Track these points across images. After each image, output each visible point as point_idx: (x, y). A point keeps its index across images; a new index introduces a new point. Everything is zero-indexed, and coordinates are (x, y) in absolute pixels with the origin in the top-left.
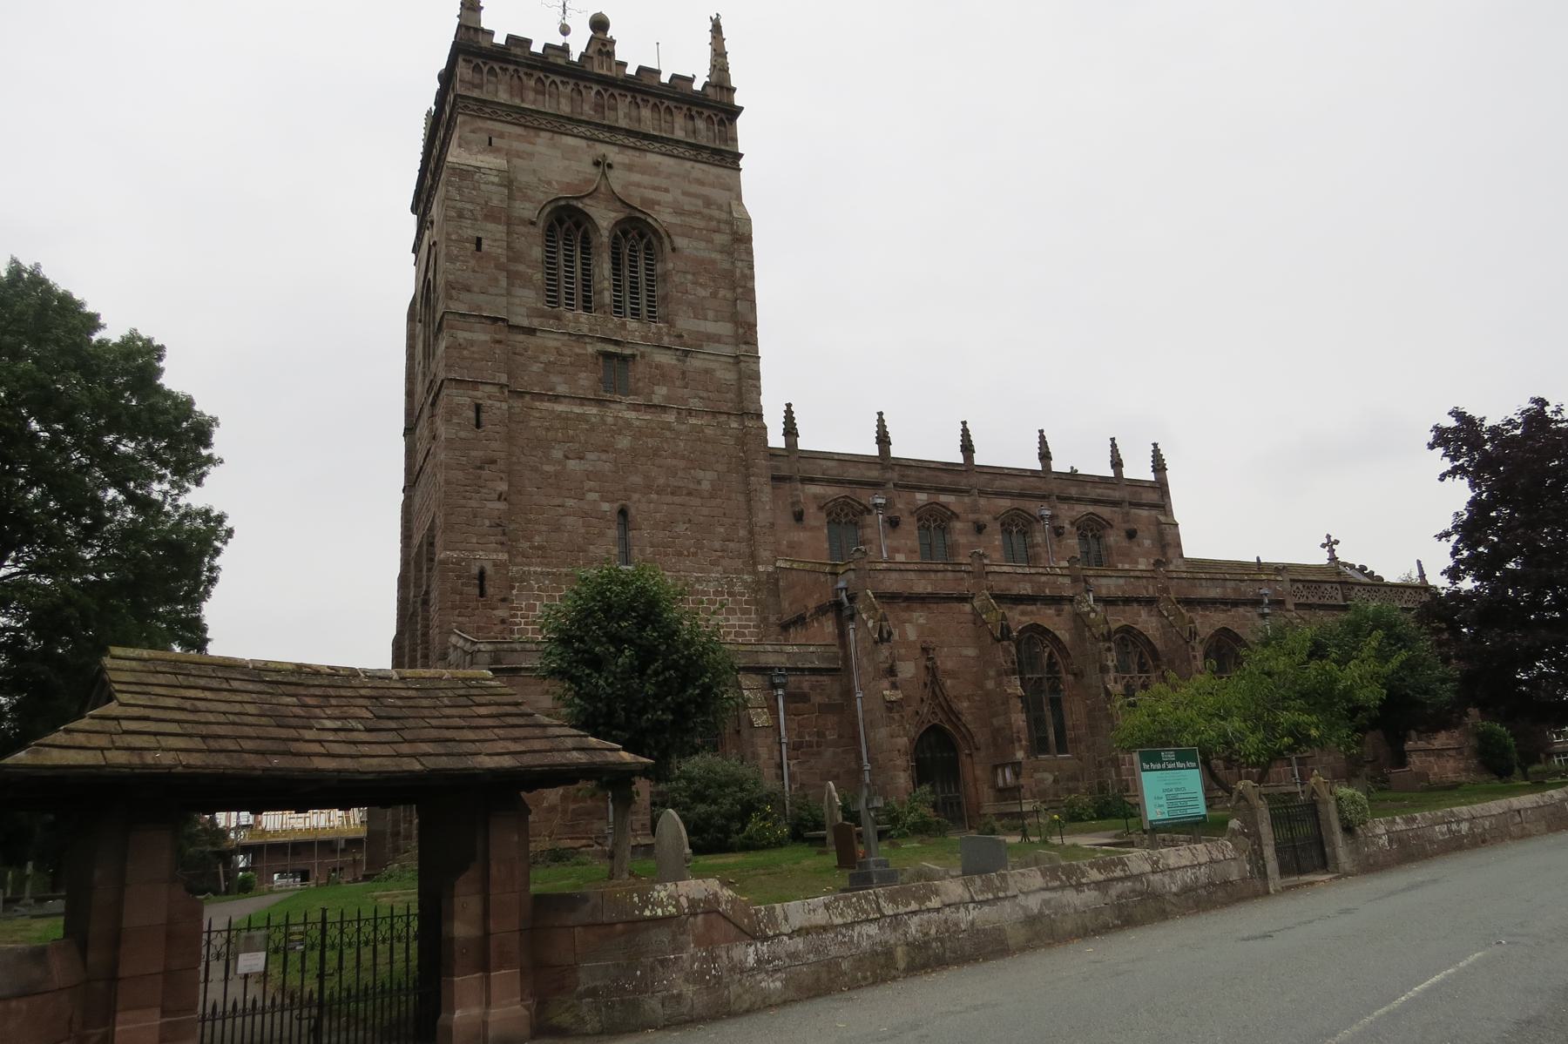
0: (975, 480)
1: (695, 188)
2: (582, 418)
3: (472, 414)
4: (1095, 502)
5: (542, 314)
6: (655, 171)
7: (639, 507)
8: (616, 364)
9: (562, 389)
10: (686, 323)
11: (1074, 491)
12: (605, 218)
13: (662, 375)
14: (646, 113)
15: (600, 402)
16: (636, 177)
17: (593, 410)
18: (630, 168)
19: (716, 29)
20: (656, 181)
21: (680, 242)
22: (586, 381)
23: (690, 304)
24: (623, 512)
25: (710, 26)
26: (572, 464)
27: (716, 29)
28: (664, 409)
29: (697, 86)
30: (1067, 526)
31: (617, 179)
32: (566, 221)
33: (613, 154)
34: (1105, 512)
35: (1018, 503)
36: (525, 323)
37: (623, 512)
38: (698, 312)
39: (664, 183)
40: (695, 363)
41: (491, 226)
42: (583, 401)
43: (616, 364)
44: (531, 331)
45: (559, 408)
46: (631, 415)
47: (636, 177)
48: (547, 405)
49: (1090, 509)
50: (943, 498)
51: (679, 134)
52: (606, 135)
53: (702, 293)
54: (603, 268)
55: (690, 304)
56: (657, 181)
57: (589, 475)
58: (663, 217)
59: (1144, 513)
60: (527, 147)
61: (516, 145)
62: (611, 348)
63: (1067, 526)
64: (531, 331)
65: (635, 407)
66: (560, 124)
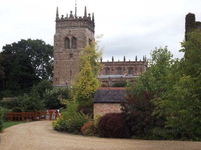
0: (113, 64)
1: (80, 32)
2: (67, 61)
3: (56, 62)
4: (131, 65)
5: (63, 50)
6: (76, 30)
7: (72, 70)
8: (71, 55)
9: (65, 58)
10: (78, 49)
11: (128, 64)
12: (70, 38)
13: (76, 55)
14: (75, 23)
15: (69, 59)
16: (74, 32)
17: (68, 60)
18: (73, 31)
19: (85, 8)
20: (76, 32)
21: (78, 39)
22: (67, 57)
23: (79, 46)
24: (71, 71)
25: (85, 7)
26: (66, 66)
27: (85, 8)
28: (76, 59)
29: (82, 17)
30: (126, 69)
31: (71, 33)
32: (67, 39)
33: (71, 30)
34: (133, 66)
35: (119, 66)
36: (62, 52)
37: (71, 71)
38: (80, 47)
39: (77, 32)
40: (79, 53)
41: (58, 42)
42: (67, 59)
43: (71, 55)
44: (62, 52)
45: (65, 60)
46: (72, 60)
47: (74, 32)
48: (64, 60)
49: (131, 66)
50: (108, 66)
51: (79, 25)
52: (70, 27)
53: (81, 45)
54: (71, 43)
55: (79, 46)
56: (76, 32)
57: (67, 67)
58: (76, 37)
59: (140, 66)
60: (62, 31)
61: (61, 31)
62: (70, 53)
63: (126, 69)
64: (62, 52)
65: (72, 59)
66: (65, 27)
